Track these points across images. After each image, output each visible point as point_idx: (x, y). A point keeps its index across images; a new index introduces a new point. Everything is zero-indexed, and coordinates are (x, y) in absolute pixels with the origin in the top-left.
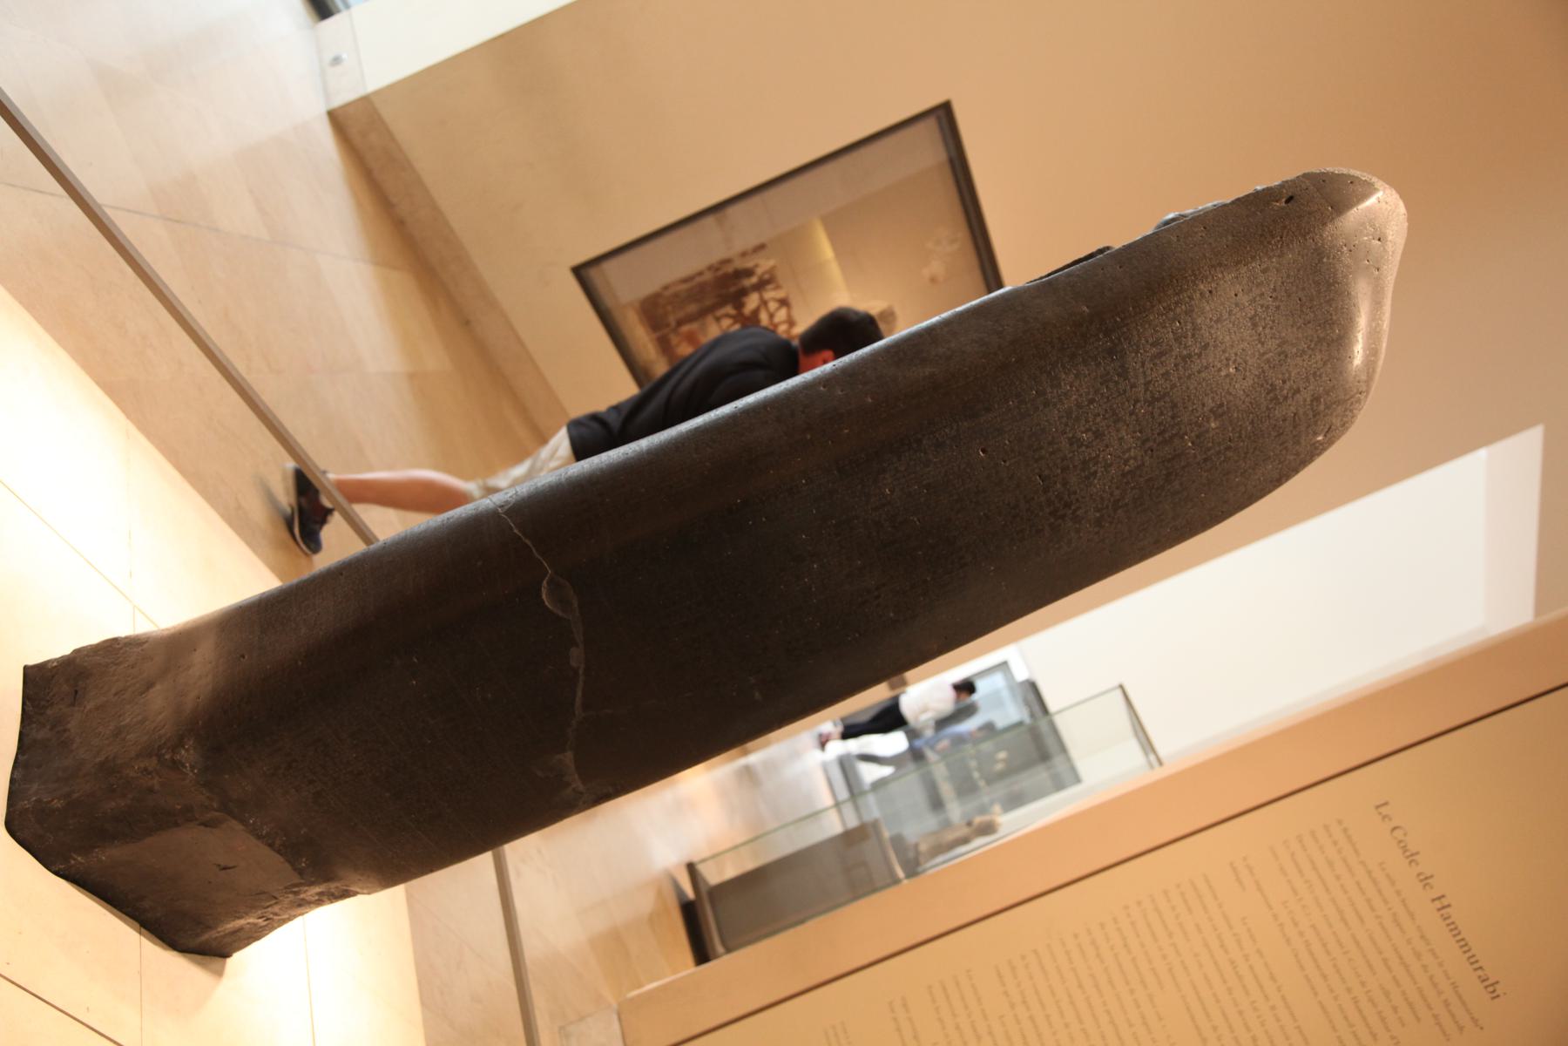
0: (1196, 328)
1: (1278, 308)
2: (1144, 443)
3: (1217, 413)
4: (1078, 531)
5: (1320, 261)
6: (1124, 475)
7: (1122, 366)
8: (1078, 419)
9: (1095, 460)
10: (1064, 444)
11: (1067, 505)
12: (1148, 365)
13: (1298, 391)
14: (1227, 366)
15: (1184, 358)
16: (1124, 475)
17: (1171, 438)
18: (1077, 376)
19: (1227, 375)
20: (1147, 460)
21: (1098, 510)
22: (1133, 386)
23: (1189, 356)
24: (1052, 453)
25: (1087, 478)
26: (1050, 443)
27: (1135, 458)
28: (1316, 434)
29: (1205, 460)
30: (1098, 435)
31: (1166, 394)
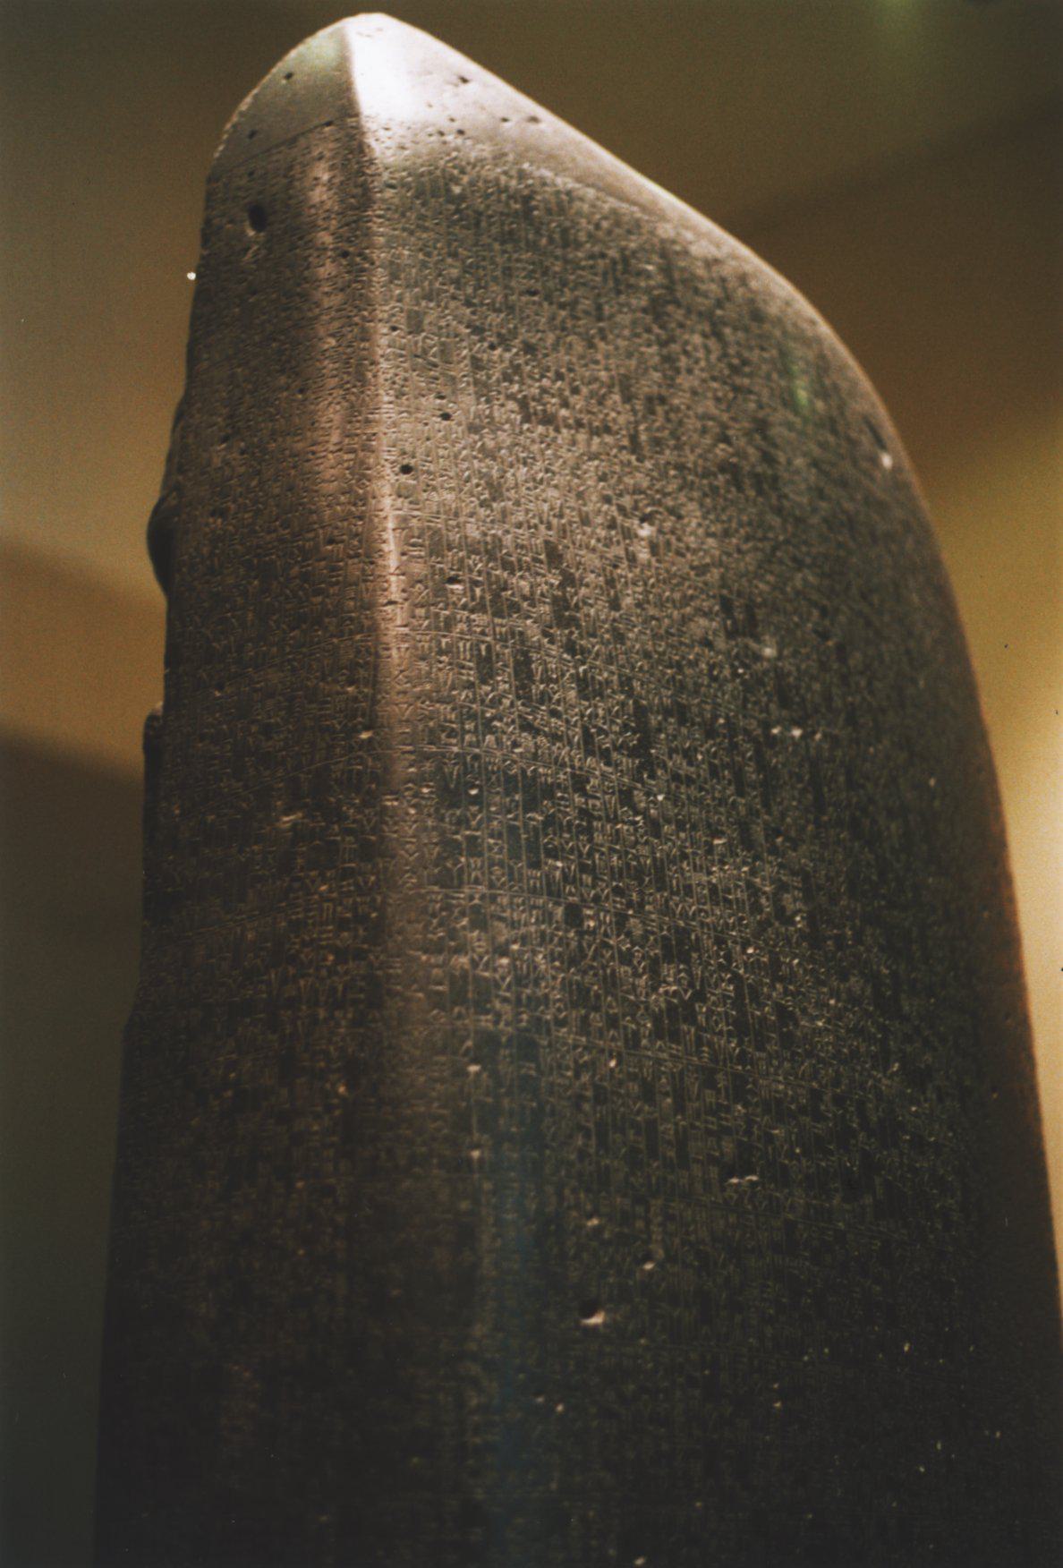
0: (491, 550)
1: (529, 348)
2: (747, 842)
3: (743, 618)
5: (452, 199)
6: (813, 938)
7: (510, 784)
8: (611, 982)
9: (746, 994)
12: (541, 716)
13: (762, 426)
14: (629, 534)
17: (762, 766)
18: (480, 922)
19: (654, 548)
20: (801, 858)
22: (579, 783)
23: (560, 604)
24: (679, 1107)
25: (787, 1040)
26: (648, 1093)
27: (782, 887)
28: (875, 461)
29: (851, 720)
30: (678, 948)
31: (641, 712)
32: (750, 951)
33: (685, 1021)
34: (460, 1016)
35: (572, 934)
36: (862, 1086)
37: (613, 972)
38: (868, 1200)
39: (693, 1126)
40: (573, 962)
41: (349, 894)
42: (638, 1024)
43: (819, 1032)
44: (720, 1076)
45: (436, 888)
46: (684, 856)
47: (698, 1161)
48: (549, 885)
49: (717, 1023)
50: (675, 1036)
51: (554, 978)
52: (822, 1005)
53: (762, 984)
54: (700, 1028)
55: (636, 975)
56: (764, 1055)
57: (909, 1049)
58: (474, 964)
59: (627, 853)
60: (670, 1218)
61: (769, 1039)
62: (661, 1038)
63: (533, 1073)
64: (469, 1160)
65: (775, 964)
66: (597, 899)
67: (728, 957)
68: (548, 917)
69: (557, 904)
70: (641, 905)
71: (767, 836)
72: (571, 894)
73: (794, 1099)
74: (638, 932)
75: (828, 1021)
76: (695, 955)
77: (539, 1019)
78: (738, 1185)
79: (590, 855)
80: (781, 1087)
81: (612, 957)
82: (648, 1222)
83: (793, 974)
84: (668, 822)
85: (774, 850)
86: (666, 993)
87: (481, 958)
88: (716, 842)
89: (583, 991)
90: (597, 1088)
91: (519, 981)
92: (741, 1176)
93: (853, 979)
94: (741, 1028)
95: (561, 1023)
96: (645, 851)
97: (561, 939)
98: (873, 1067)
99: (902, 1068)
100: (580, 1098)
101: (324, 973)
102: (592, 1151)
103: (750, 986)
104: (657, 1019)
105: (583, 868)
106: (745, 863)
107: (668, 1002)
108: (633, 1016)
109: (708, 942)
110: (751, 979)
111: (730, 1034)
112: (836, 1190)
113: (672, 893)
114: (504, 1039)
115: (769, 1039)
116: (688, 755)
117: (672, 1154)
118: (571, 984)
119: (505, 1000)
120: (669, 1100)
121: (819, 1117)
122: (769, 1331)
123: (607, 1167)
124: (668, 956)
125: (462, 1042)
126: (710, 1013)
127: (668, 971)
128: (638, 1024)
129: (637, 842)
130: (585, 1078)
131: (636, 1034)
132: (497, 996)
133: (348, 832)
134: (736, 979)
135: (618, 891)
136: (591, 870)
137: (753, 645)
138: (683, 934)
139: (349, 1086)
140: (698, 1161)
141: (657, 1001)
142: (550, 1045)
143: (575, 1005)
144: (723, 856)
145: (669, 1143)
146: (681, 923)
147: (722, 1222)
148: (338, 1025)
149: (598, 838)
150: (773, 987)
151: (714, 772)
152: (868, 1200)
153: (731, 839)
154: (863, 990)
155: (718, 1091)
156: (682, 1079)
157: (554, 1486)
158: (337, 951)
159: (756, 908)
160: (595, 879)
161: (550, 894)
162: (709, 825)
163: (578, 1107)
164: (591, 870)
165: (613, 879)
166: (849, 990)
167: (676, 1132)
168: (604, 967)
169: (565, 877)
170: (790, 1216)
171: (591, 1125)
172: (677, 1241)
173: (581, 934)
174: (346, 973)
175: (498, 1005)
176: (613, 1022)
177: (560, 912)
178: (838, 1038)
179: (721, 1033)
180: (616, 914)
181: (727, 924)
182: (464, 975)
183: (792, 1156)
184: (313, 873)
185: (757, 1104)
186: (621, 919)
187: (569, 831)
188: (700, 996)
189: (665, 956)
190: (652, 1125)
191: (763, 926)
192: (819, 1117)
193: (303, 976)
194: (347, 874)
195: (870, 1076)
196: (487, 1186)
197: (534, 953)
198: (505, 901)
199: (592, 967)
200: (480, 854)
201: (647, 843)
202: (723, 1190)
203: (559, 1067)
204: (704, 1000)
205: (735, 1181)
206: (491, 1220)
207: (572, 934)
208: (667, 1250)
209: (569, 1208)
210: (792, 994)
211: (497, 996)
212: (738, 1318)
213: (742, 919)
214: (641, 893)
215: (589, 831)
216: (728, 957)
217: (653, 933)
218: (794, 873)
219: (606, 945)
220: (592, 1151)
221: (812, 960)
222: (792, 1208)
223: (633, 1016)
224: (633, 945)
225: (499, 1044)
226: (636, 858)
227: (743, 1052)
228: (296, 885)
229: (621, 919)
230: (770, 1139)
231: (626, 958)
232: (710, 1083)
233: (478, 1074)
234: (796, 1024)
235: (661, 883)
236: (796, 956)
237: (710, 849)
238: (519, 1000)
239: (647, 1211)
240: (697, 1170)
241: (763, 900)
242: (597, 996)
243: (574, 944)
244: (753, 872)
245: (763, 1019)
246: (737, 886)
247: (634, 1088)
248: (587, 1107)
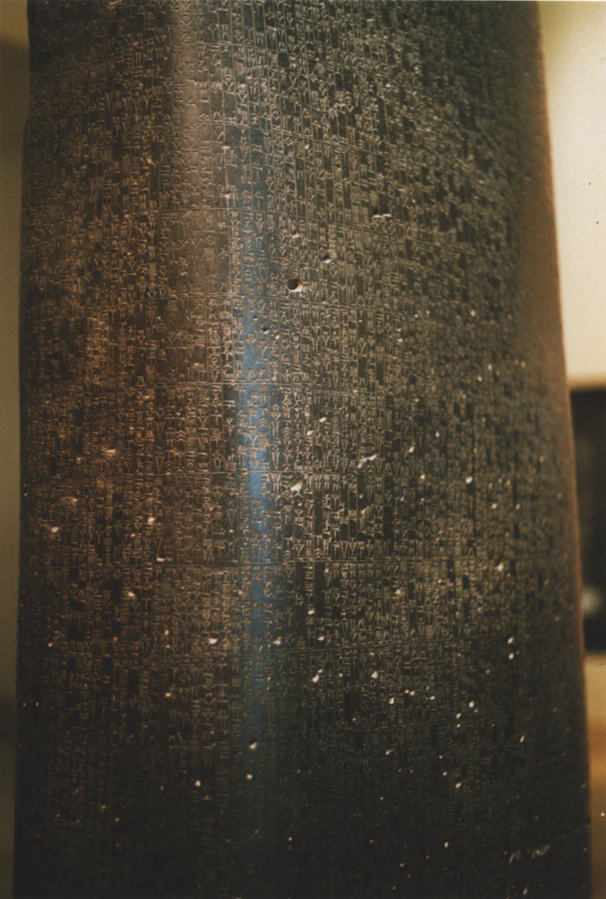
2: (387, 21)
6: (425, 81)
8: (306, 100)
9: (385, 110)
11: (440, 195)
16: (425, 81)
18: (229, 62)
20: (418, 32)
21: (464, 153)
24: (346, 174)
25: (409, 138)
26: (327, 165)
27: (407, 49)
32: (388, 86)
33: (349, 124)
34: (217, 118)
35: (282, 71)
36: (452, 167)
37: (307, 94)
38: (453, 231)
39: (353, 185)
40: (283, 87)
41: (151, 46)
42: (322, 125)
43: (427, 135)
44: (369, 157)
45: (202, 42)
46: (349, 28)
47: (356, 204)
48: (269, 41)
49: (368, 126)
50: (343, 133)
51: (272, 96)
52: (429, 119)
53: (395, 105)
54: (358, 129)
55: (321, 96)
56: (395, 146)
57: (479, 147)
58: (225, 87)
59: (315, 24)
60: (340, 235)
61: (398, 137)
62: (335, 133)
63: (261, 151)
64: (224, 200)
65: (403, 94)
66: (297, 51)
67: (375, 88)
68: (269, 61)
69: (274, 53)
70: (324, 55)
71: (399, 18)
72: (282, 47)
73: (412, 172)
74: (322, 71)
75: (433, 129)
76: (355, 87)
77: (264, 120)
78: (379, 219)
79: (293, 24)
80: (405, 165)
81: (307, 85)
82: (327, 237)
83: (413, 100)
84: (340, 7)
85: (403, 27)
86: (338, 108)
87: (229, 84)
88: (369, 20)
89: (290, 105)
90: (297, 160)
91: (251, 98)
92: (381, 214)
93: (448, 105)
94: (382, 129)
95: (277, 123)
96: (326, 23)
97: (276, 74)
98: (459, 157)
99: (476, 158)
100: (288, 165)
101: (137, 93)
102: (295, 196)
103: (388, 106)
104: (333, 122)
105: (289, 33)
106: (385, 34)
107: (339, 113)
108: (319, 120)
109: (363, 79)
110: (388, 102)
111: (375, 133)
112: (435, 224)
113: (342, 49)
114: (243, 131)
115: (398, 137)
117: (341, 199)
118: (282, 100)
119: (244, 109)
120: (340, 169)
121: (426, 183)
122: (396, 300)
123: (304, 205)
124: (340, 86)
125: (219, 133)
126: (364, 121)
127: (340, 95)
128: (322, 125)
129: (321, 18)
130: (291, 155)
131: (320, 130)
132: (239, 106)
133: (151, 9)
134: (380, 102)
135: (309, 46)
136: (294, 34)
138: (349, 73)
139: (153, 158)
140: (356, 204)
141: (333, 112)
142: (270, 135)
143: (285, 113)
144: (372, 29)
145: (340, 193)
146: (347, 67)
147: (370, 239)
148: (147, 124)
149: (298, 14)
150: (401, 107)
152: (453, 231)
153: (377, 19)
154: (453, 113)
155: (368, 165)
156: (347, 158)
157: (274, 379)
158: (144, 81)
159: (392, 61)
160: (296, 39)
161: (269, 47)
162: (364, 10)
163: (287, 171)
164: (294, 34)
165: (307, 39)
166: (445, 112)
167: (344, 187)
168: (302, 91)
169: (278, 37)
170: (409, 238)
171: (294, 181)
172: (344, 248)
173: (288, 71)
174: (150, 93)
175: (239, 111)
176: (307, 123)
177: (275, 58)
178: (438, 138)
179: (370, 132)
180: (309, 60)
181: (374, 69)
182: (220, 94)
183: (410, 203)
184: (129, 35)
185: (390, 174)
186: (312, 63)
187: (281, 10)
188: (358, 110)
189: (337, 87)
190: (330, 183)
191: (396, 71)
192: (426, 183)
193: (125, 96)
194: (149, 34)
195: (456, 161)
196: (235, 214)
197: (260, 81)
198: (243, 50)
199: (294, 91)
200: (227, 22)
201: (327, 19)
202: (370, 221)
203: (276, 148)
204: (360, 113)
205: (377, 216)
206: (237, 234)
207: (282, 71)
208: (338, 255)
209: (282, 228)
210: (412, 112)
211: (239, 106)
212: (378, 292)
213: (383, 67)
214: (324, 48)
215: (292, 10)
216: (375, 88)
217: (331, 72)
218: (415, 42)
219: (303, 78)
220: (295, 196)
221: (424, 92)
222: (410, 233)
223: (319, 120)
224: (319, 78)
225: (240, 134)
226: (321, 27)
227: (383, 145)
228: (119, 43)
229: (312, 63)
230: (398, 194)
231: (315, 86)
232: (364, 160)
233: (228, 151)
234: (414, 130)
235: (336, 43)
236: (415, 90)
237: (365, 24)
238: (252, 108)
239: (327, 231)
240: (356, 210)
241: (396, 56)
242: (298, 108)
243: (284, 77)
244: (390, 39)
245: (395, 126)
246: (381, 47)
247: (320, 161)
248: (292, 171)
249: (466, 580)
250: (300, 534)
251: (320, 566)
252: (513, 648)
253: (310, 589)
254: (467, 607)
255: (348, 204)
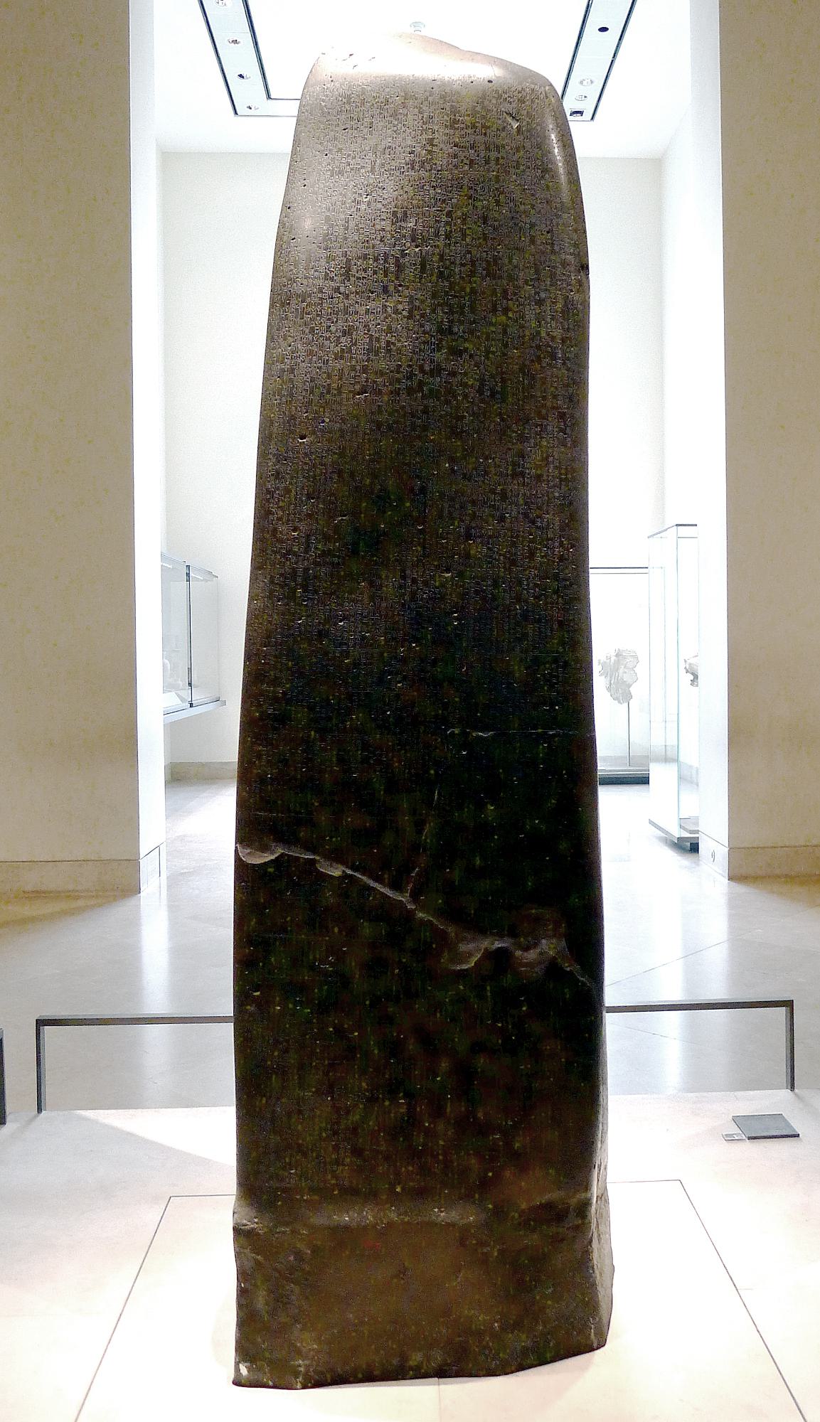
4: (453, 374)
7: (298, 296)
8: (321, 347)
10: (338, 365)
11: (410, 376)
15: (324, 240)
26: (329, 376)
31: (348, 261)
116: (365, 270)
137: (403, 224)
151: (375, 272)
249: (414, 581)
250: (295, 554)
251: (306, 570)
252: (456, 619)
253: (299, 580)
254: (413, 594)
255: (340, 393)
